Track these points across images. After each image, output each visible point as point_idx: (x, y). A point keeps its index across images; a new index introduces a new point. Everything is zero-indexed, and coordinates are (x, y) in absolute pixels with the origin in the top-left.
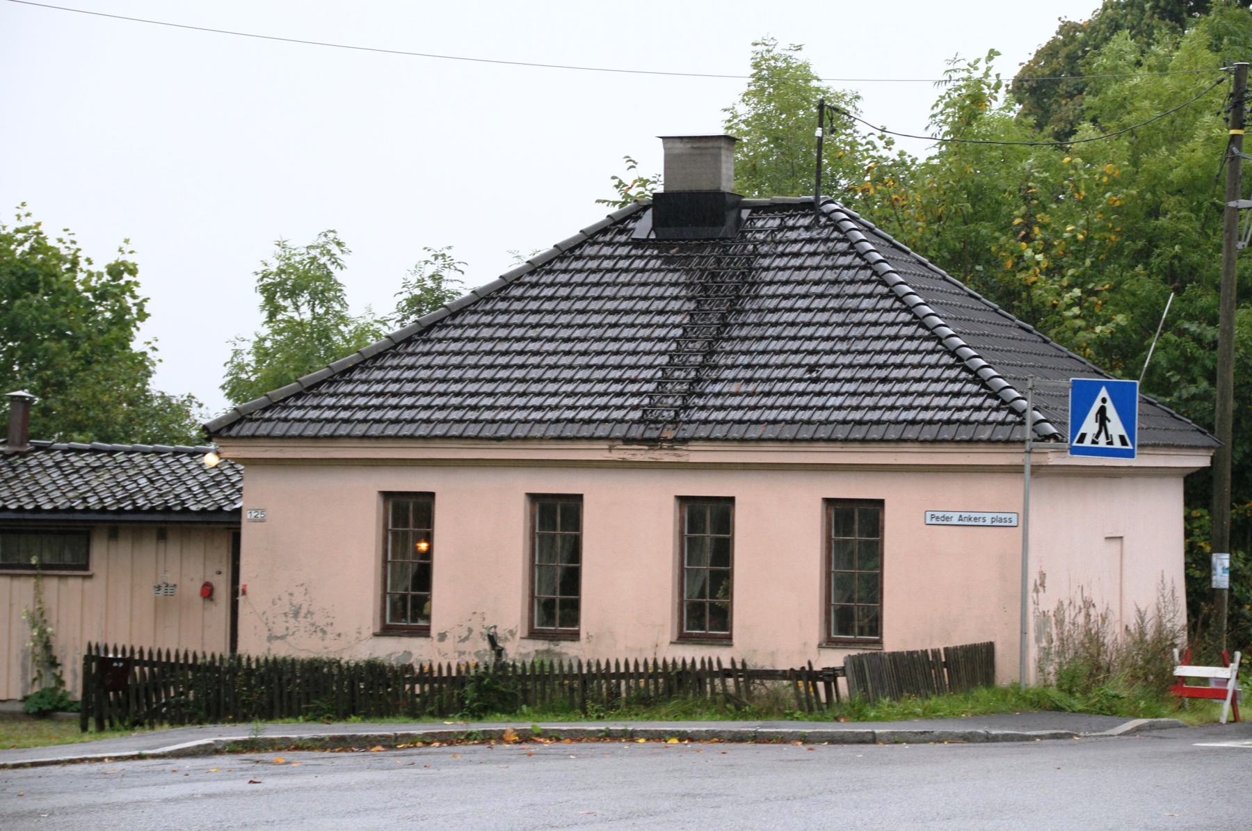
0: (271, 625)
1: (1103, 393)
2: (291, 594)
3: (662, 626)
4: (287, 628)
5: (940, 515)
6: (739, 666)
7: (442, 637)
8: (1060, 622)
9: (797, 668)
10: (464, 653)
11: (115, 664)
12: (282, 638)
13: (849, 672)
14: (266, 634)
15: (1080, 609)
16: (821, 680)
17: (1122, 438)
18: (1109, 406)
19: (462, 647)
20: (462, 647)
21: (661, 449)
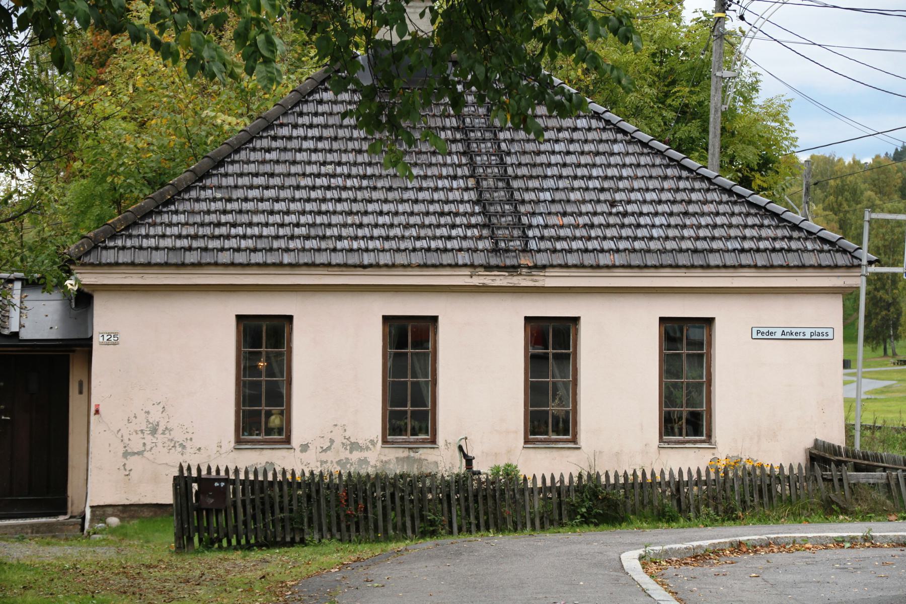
0: (126, 441)
2: (148, 413)
3: (516, 432)
4: (144, 444)
5: (765, 330)
7: (305, 448)
10: (326, 462)
11: (216, 484)
12: (138, 453)
14: (122, 450)
19: (324, 457)
20: (324, 457)
21: (520, 274)
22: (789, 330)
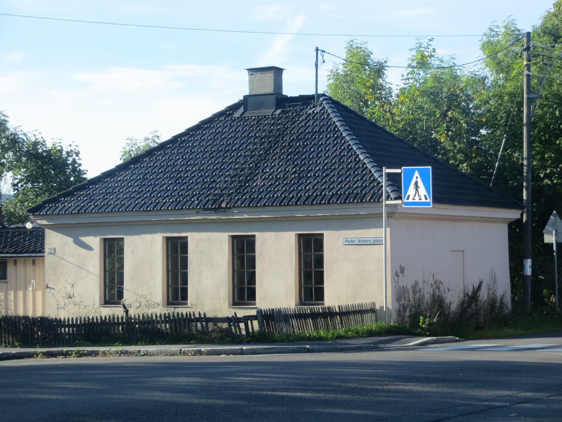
1: (417, 174)
5: (349, 240)
6: (202, 316)
8: (415, 292)
9: (230, 316)
13: (260, 318)
16: (241, 322)
17: (425, 196)
18: (419, 180)
22: (362, 239)
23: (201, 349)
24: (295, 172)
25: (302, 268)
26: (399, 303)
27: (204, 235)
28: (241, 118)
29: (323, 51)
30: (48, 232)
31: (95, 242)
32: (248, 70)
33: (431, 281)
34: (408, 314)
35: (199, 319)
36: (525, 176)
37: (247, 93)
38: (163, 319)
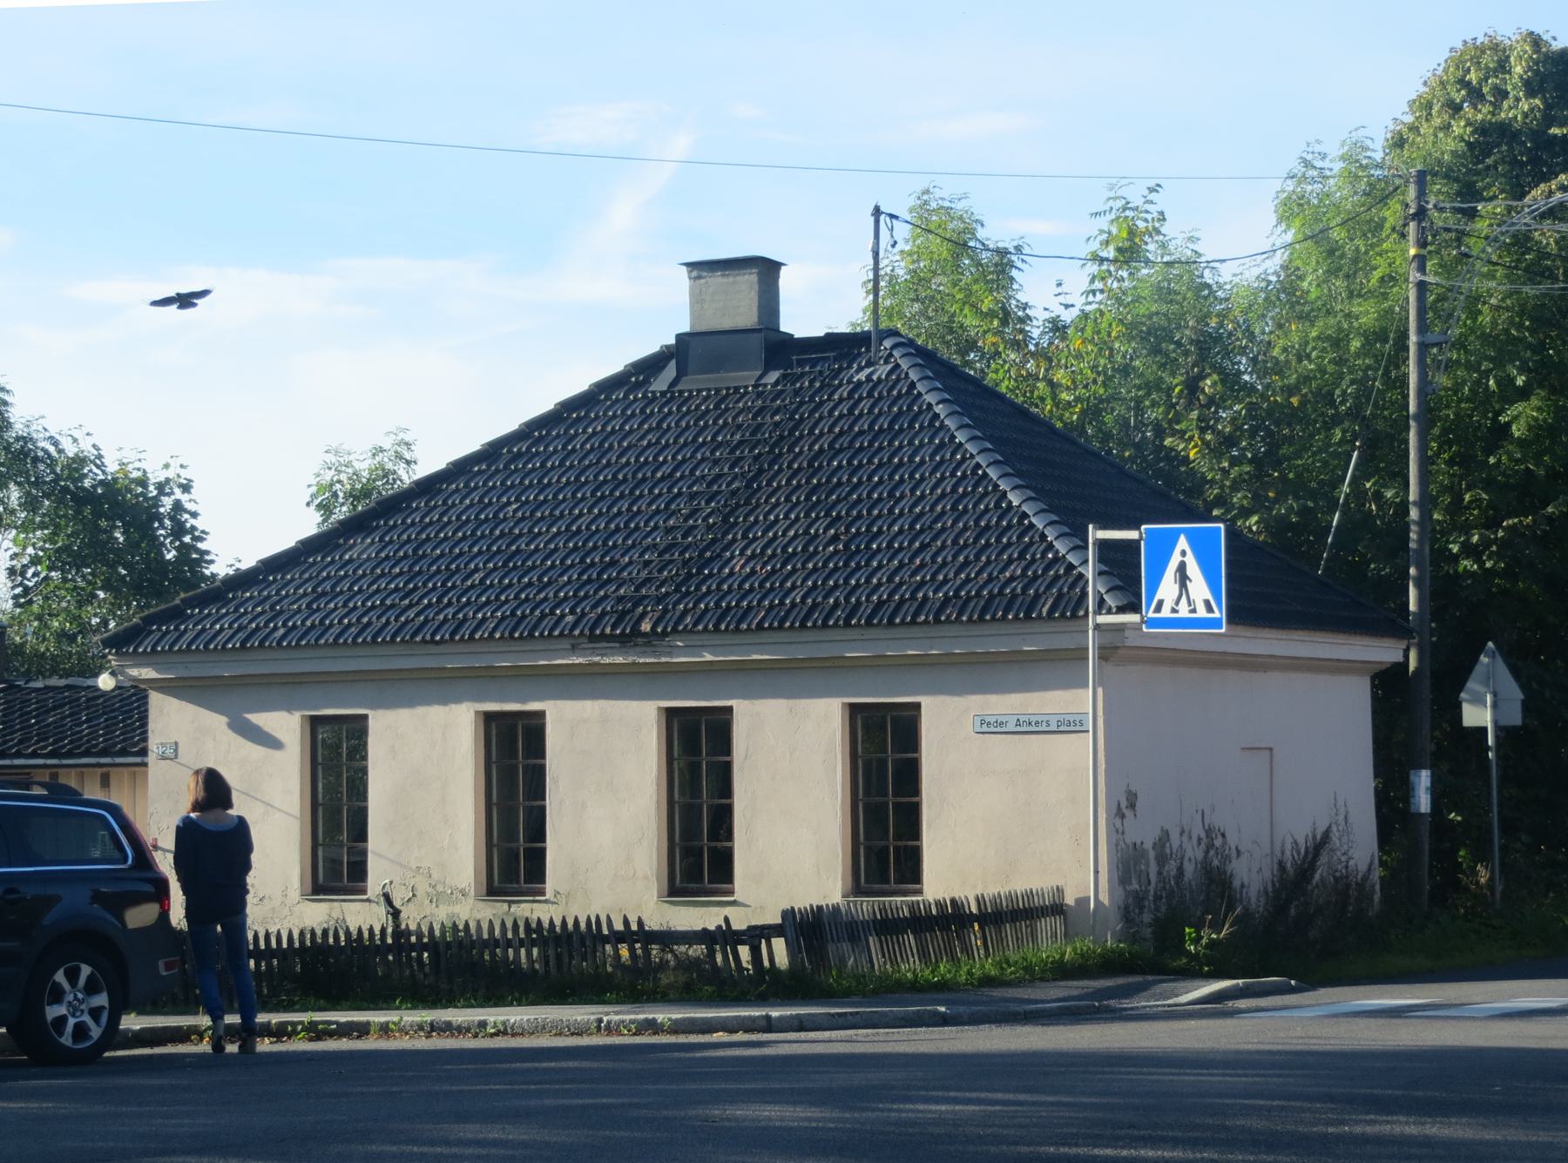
1: (1183, 543)
6: (634, 927)
8: (1162, 859)
9: (712, 927)
13: (789, 931)
15: (1200, 839)
16: (743, 943)
17: (1207, 603)
18: (1191, 561)
21: (636, 645)
22: (1025, 718)
23: (656, 1016)
24: (835, 538)
25: (861, 796)
26: (1125, 889)
27: (589, 709)
28: (670, 395)
29: (892, 216)
30: (156, 700)
31: (286, 725)
32: (687, 265)
33: (1198, 831)
34: (1147, 917)
35: (626, 936)
36: (1415, 551)
37: (685, 328)
38: (522, 935)
